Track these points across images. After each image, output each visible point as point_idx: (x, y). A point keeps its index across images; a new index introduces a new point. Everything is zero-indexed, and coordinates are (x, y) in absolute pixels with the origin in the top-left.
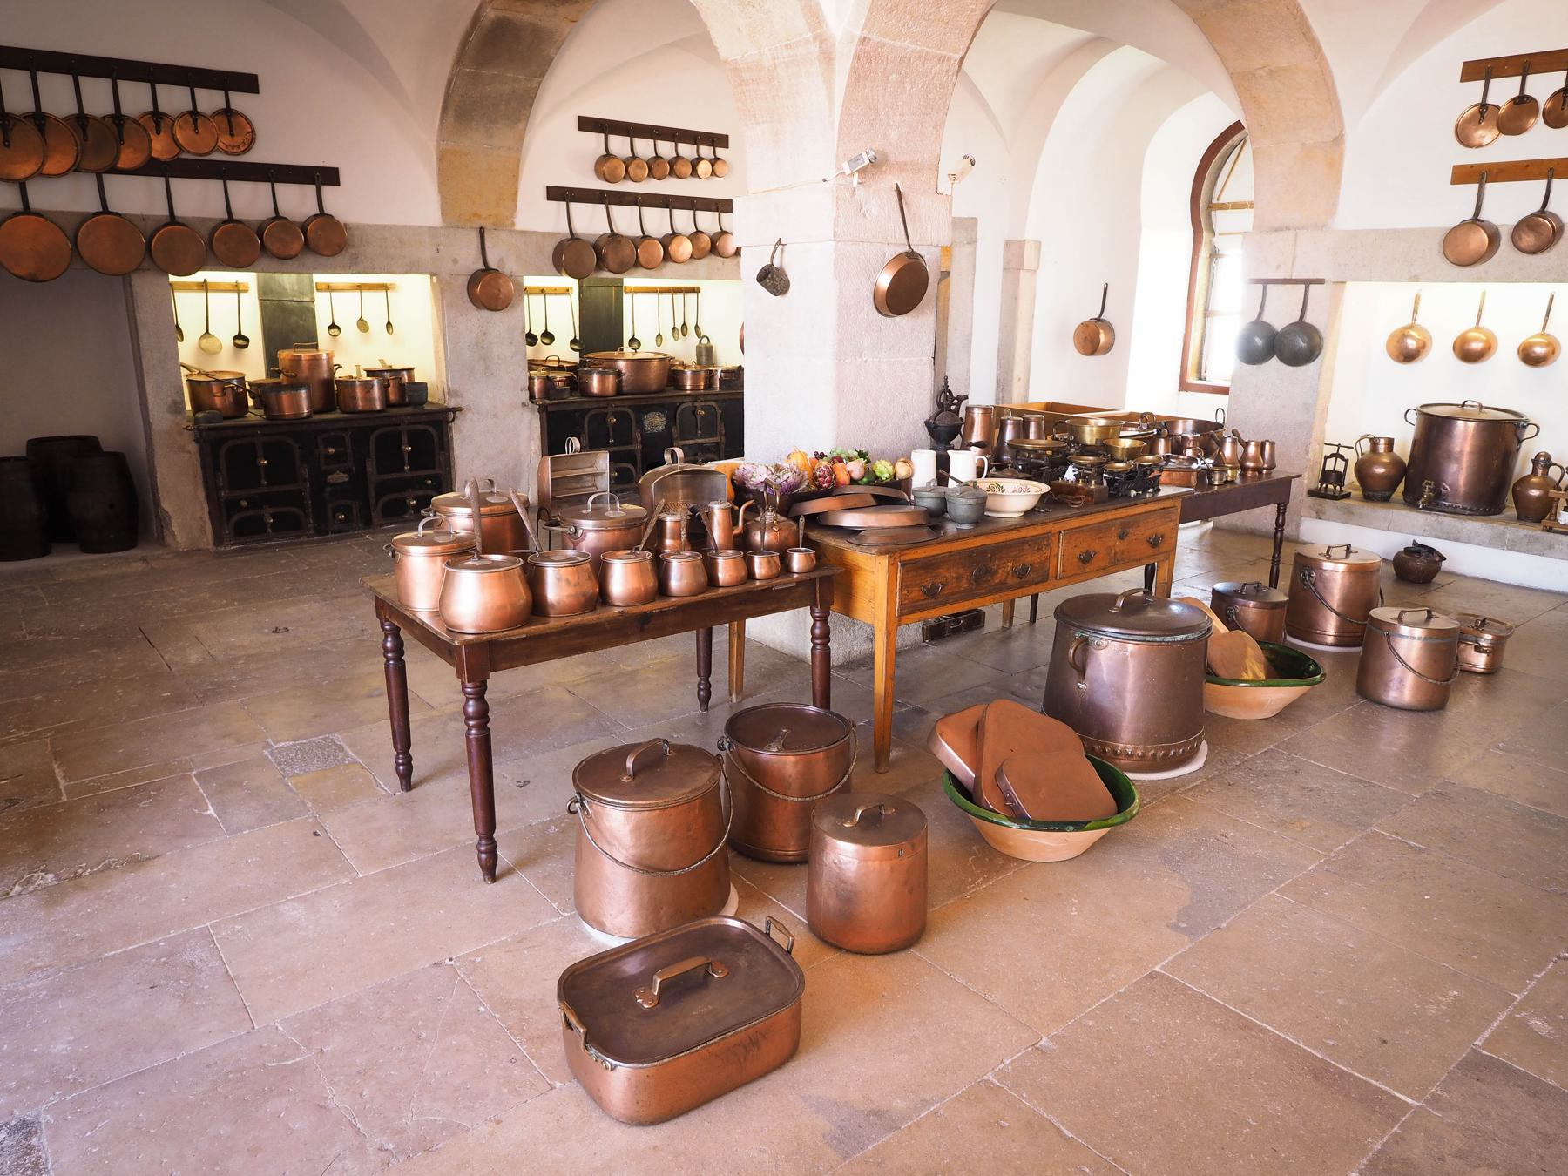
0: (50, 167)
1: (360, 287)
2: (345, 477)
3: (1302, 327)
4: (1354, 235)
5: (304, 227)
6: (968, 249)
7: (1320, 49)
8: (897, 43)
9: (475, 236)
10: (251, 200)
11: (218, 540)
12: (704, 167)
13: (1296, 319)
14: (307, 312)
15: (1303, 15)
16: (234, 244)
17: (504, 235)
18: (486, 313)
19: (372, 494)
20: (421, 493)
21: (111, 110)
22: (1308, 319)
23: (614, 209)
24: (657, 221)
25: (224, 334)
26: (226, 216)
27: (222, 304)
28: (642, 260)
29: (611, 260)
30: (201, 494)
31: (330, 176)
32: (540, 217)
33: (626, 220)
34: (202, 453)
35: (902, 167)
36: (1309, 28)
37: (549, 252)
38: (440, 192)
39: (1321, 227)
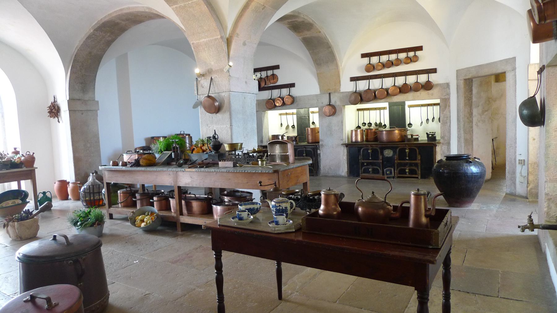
6: (513, 73)
8: (201, 41)
9: (328, 95)
17: (336, 94)
27: (290, 117)
31: (292, 85)
32: (347, 87)
38: (319, 85)
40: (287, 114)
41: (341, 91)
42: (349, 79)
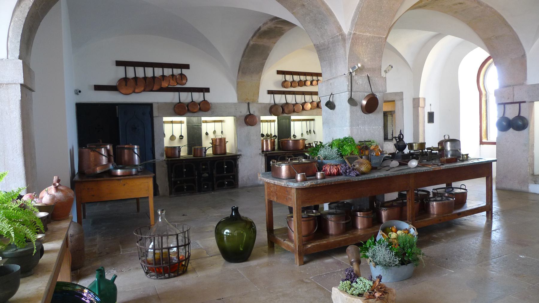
0: (137, 91)
1: (215, 121)
2: (207, 175)
3: (519, 117)
4: (534, 85)
5: (199, 104)
6: (401, 102)
7: (512, 28)
8: (365, 34)
9: (246, 105)
10: (185, 97)
11: (171, 193)
12: (314, 83)
13: (517, 115)
14: (200, 129)
15: (504, 19)
16: (180, 109)
18: (249, 127)
19: (215, 180)
20: (229, 180)
21: (152, 75)
22: (522, 115)
23: (287, 96)
24: (300, 99)
25: (177, 136)
26: (178, 101)
27: (177, 127)
28: (295, 110)
29: (286, 111)
30: (167, 179)
31: (207, 90)
32: (265, 99)
33: (290, 99)
34: (168, 167)
35: (369, 70)
36: (507, 22)
37: (268, 109)
39: (522, 84)
40: (172, 122)
41: (259, 102)
42: (266, 92)
